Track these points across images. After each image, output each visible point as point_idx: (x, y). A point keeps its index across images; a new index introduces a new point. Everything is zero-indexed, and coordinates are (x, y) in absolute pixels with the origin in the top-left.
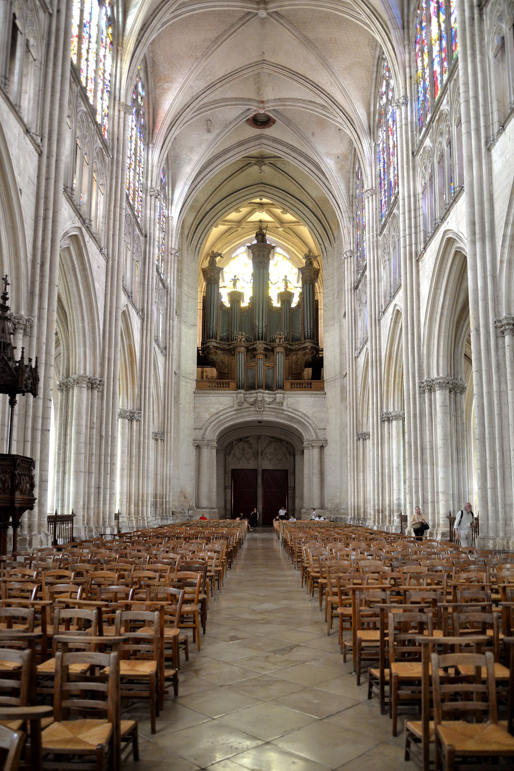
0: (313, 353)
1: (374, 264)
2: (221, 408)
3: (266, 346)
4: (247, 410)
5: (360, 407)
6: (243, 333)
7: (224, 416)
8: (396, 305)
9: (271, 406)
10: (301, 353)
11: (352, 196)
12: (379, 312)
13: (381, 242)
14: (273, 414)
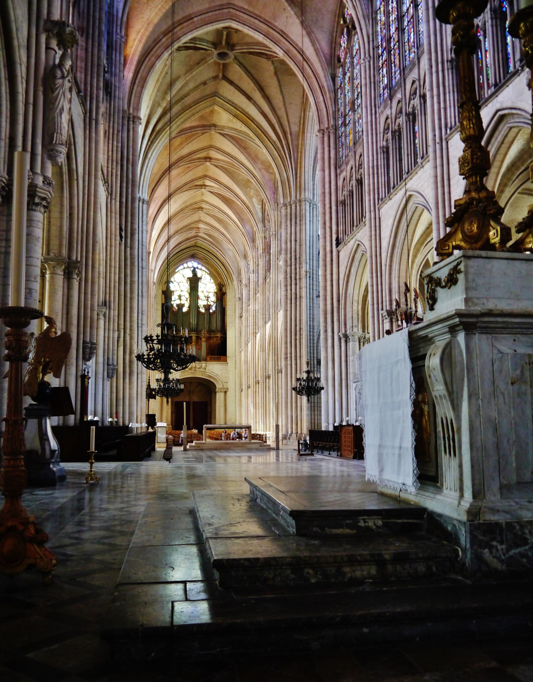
10: (215, 339)
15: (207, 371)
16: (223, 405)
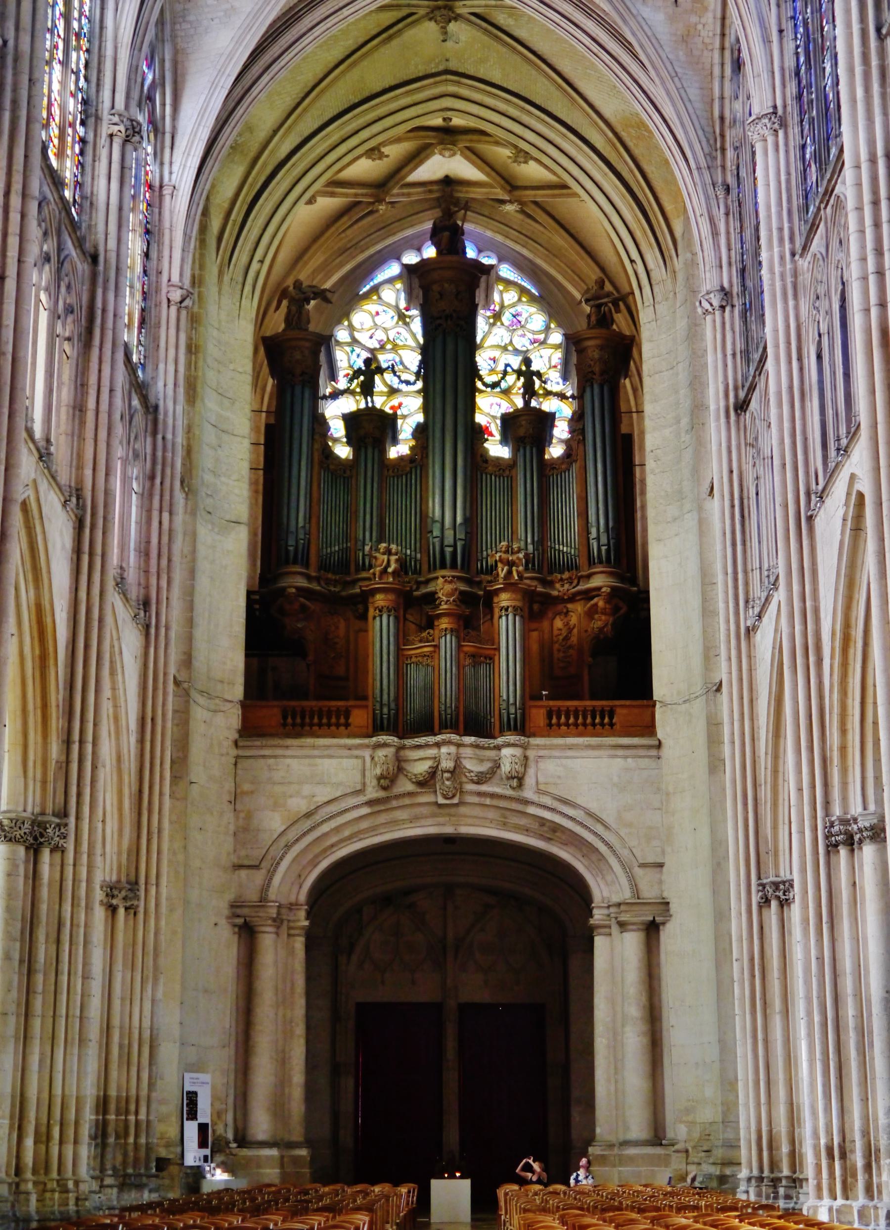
0: (616, 609)
1: (788, 343)
2: (323, 794)
3: (463, 587)
4: (407, 801)
5: (765, 793)
6: (394, 547)
7: (333, 824)
8: (853, 477)
9: (484, 788)
10: (578, 609)
11: (722, 118)
12: (808, 494)
13: (805, 278)
14: (491, 814)
15: (528, 793)
16: (634, 1010)
